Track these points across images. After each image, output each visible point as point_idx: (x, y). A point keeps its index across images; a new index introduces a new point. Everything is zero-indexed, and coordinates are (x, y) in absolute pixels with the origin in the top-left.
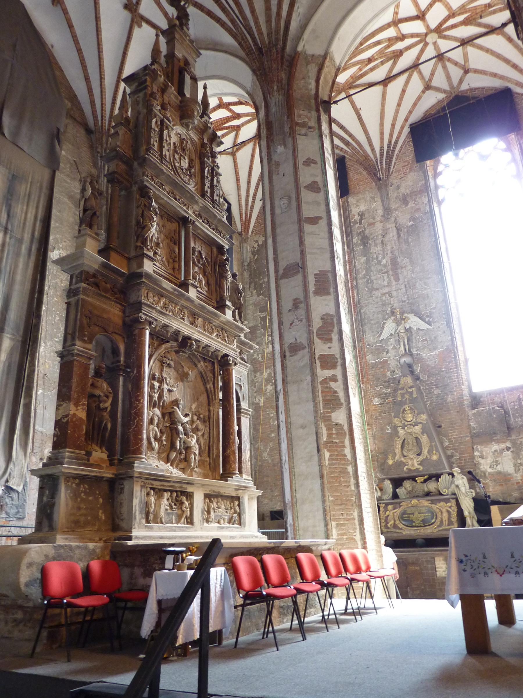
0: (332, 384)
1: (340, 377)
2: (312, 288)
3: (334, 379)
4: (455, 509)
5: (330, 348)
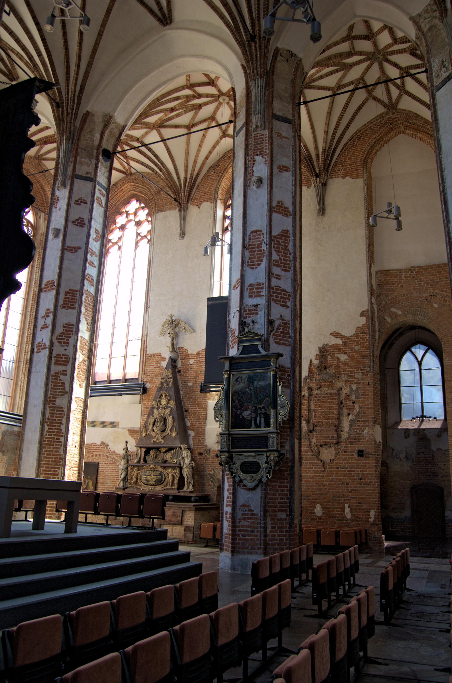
0: (62, 377)
1: (69, 373)
2: (61, 302)
3: (64, 373)
4: (178, 474)
5: (65, 350)
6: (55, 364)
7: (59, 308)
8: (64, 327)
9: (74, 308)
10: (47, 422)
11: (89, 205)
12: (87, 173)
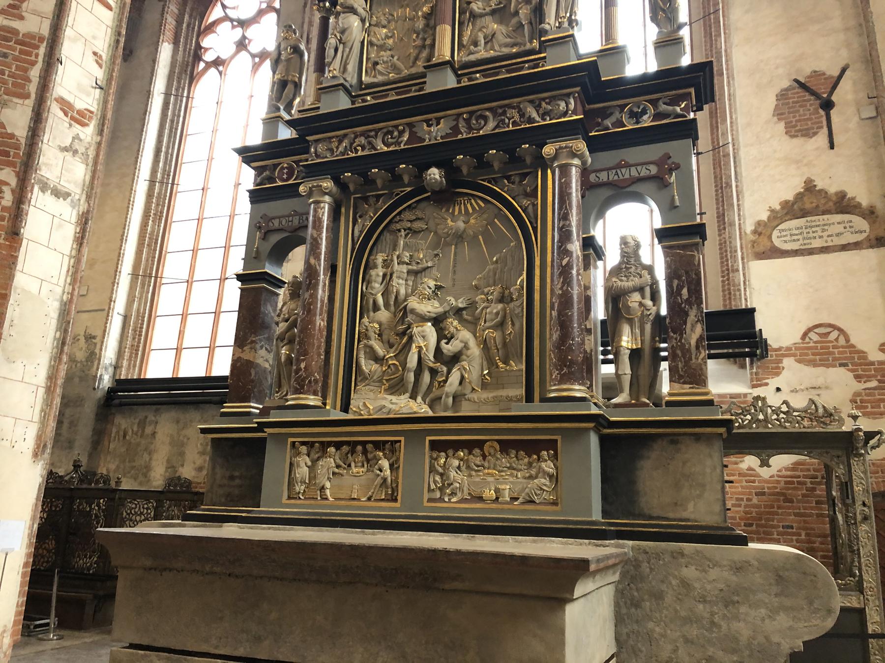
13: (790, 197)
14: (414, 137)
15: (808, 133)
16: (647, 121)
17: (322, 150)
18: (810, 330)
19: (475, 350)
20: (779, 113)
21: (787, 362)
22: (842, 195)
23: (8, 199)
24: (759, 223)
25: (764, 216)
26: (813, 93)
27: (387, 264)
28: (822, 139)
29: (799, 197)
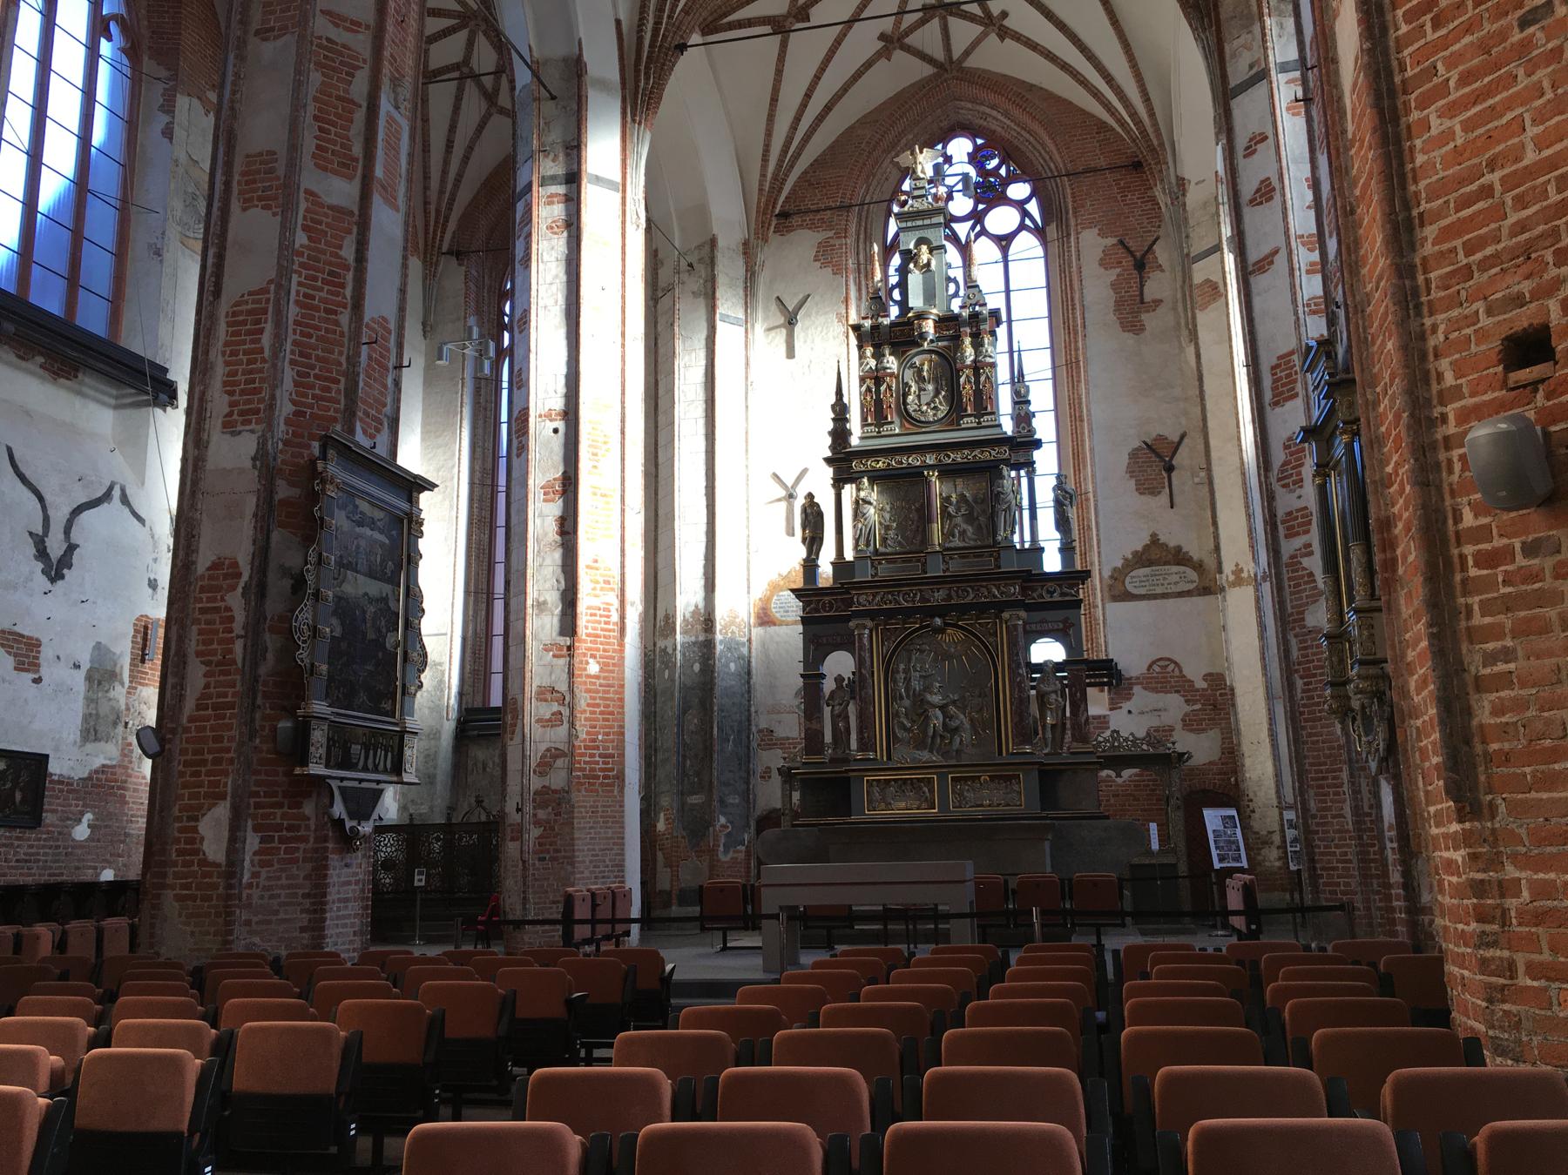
0: (1306, 562)
2: (1268, 396)
6: (1286, 537)
7: (1268, 408)
8: (1286, 447)
9: (1296, 395)
10: (1297, 671)
11: (1271, 140)
12: (1251, 67)
13: (1139, 548)
14: (923, 599)
15: (1153, 491)
16: (1056, 597)
17: (863, 601)
18: (1154, 663)
19: (967, 726)
20: (1131, 472)
21: (1137, 689)
22: (1179, 549)
23: (615, 617)
24: (1115, 569)
25: (1119, 564)
26: (1158, 455)
27: (906, 671)
28: (1164, 498)
29: (1147, 548)
